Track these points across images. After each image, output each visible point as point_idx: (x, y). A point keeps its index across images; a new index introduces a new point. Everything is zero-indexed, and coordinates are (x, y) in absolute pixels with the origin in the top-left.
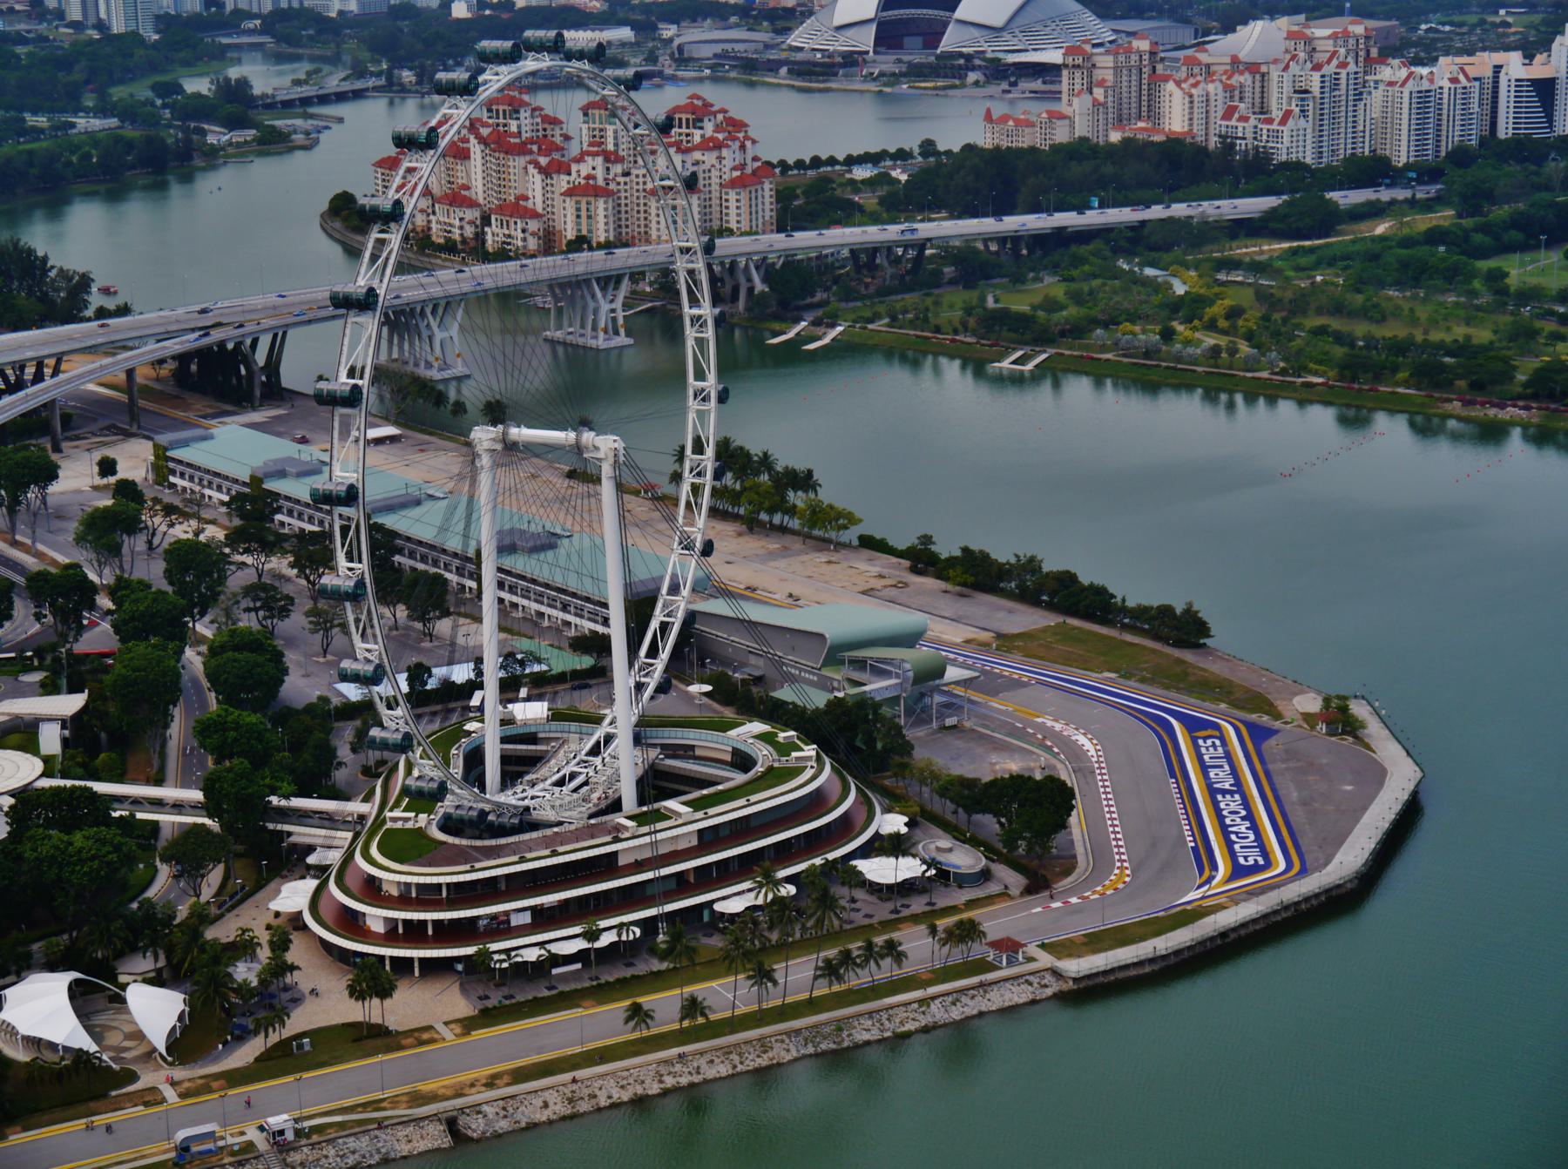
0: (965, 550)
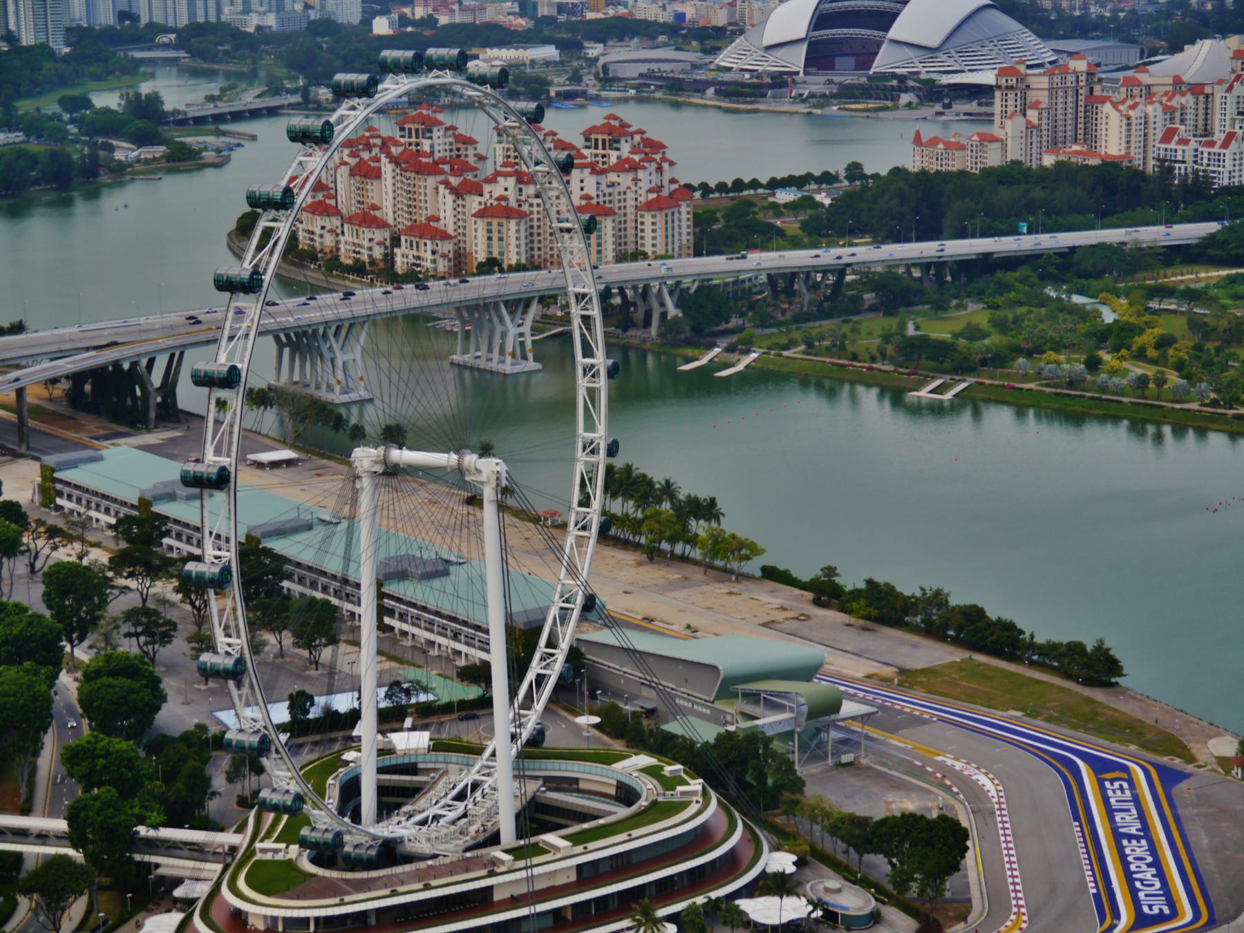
0: (870, 582)
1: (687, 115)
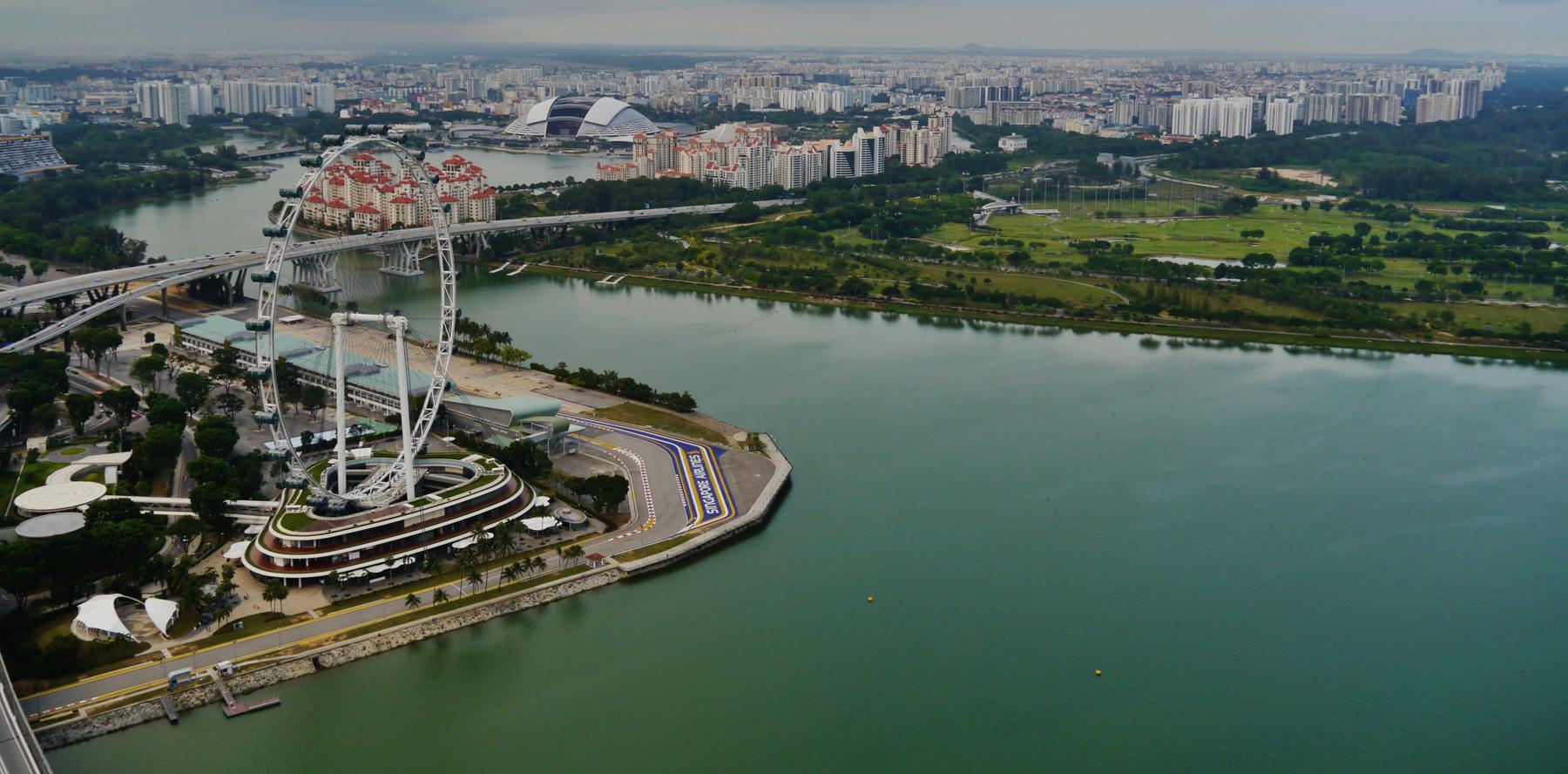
0: (686, 395)
1: (491, 154)
